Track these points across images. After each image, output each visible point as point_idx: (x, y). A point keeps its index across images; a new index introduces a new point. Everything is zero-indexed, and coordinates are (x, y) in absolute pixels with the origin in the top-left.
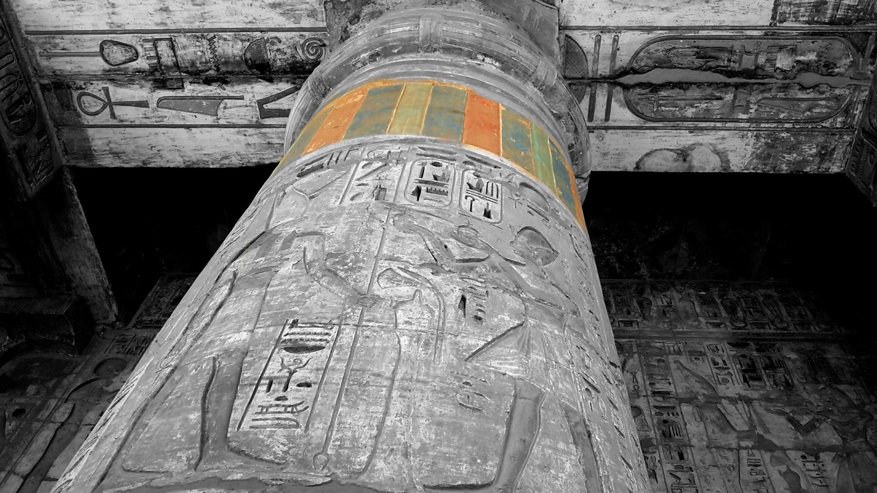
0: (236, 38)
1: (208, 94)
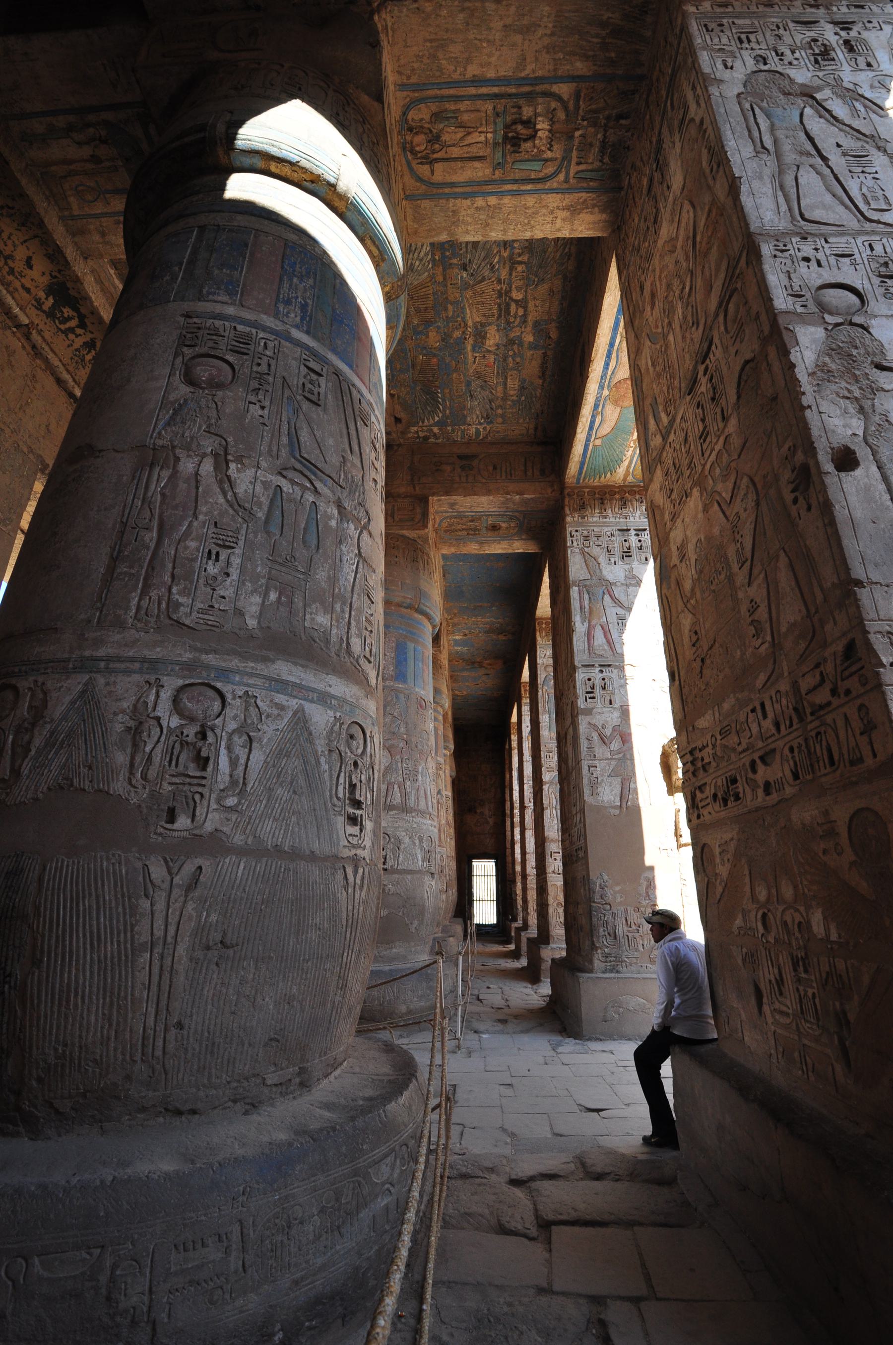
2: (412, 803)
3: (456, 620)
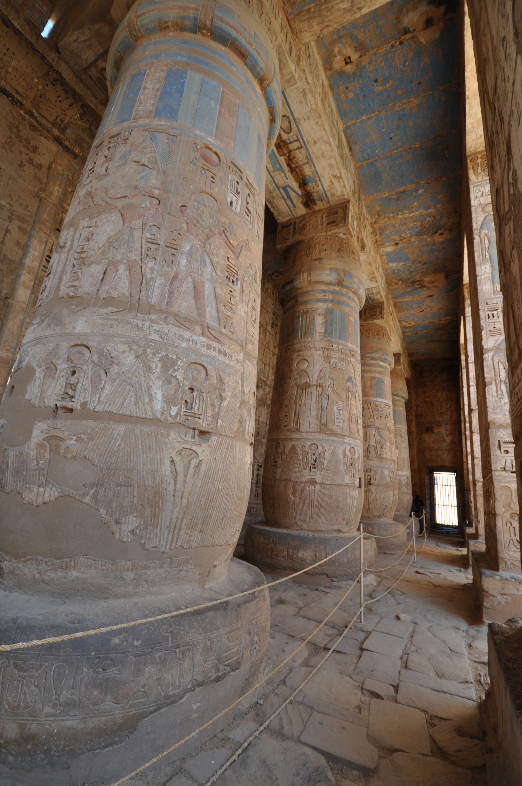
0: (313, 172)
1: (283, 166)
2: (155, 295)
3: (381, 223)
